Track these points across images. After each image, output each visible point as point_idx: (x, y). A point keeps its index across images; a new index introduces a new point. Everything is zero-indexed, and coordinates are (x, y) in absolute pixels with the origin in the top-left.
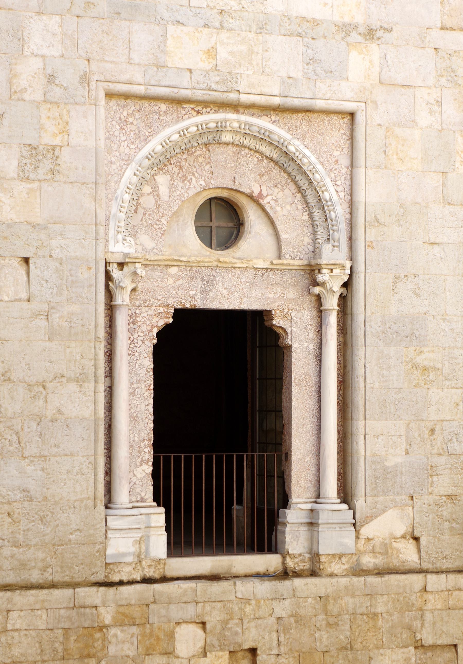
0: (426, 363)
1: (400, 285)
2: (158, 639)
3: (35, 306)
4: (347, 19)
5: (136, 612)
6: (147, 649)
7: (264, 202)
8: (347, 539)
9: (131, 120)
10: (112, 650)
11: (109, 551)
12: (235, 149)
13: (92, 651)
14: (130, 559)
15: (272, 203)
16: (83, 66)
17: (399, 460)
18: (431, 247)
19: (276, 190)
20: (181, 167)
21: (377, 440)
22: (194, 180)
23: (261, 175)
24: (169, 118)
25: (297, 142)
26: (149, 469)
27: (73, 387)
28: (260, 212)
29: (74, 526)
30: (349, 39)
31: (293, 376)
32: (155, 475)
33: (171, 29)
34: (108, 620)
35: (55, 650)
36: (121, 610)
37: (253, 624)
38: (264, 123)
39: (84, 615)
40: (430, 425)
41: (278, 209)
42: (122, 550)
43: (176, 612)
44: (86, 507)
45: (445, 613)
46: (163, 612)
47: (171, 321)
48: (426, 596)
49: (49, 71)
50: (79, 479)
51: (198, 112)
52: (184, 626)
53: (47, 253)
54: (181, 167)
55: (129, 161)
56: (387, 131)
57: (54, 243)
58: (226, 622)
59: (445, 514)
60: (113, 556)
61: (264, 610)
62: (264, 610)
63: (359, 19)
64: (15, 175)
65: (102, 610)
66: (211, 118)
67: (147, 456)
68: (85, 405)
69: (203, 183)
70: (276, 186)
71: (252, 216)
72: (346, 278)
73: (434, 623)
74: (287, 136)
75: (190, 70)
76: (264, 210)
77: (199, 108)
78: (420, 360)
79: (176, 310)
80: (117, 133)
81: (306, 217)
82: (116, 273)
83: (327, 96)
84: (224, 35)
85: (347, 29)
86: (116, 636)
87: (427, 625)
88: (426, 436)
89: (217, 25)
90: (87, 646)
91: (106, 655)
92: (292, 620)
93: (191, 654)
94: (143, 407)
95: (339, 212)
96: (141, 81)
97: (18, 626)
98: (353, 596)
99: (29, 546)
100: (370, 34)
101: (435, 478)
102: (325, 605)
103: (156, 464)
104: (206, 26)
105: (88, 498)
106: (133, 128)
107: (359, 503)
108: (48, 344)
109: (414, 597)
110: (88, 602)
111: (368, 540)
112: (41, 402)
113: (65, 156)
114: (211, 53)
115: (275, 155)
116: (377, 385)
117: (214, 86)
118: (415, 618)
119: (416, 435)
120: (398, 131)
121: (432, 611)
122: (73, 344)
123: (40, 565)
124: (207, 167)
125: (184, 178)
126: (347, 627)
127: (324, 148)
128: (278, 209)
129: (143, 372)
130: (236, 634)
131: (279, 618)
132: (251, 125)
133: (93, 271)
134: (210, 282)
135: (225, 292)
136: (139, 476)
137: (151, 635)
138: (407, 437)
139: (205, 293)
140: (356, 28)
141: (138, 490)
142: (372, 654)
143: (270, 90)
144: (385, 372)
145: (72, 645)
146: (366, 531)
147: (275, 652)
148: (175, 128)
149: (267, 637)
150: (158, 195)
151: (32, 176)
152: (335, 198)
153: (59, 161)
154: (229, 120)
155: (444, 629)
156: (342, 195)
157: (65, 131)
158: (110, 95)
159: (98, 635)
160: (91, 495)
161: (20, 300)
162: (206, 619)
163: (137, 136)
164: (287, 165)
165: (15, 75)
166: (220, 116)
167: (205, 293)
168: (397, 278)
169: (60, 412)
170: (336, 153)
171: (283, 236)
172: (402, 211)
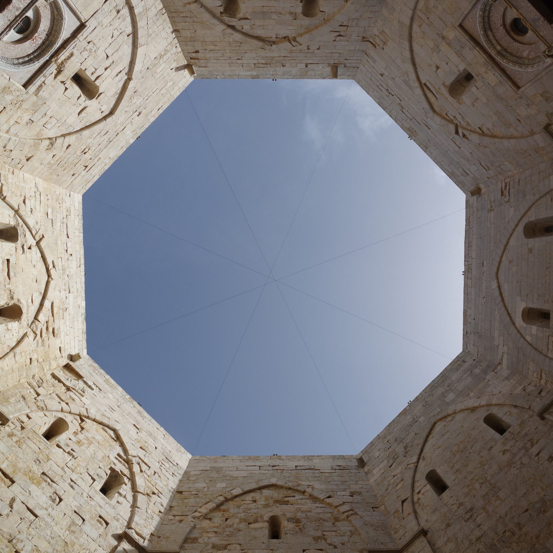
4: (448, 46)
63: (444, 43)
84: (480, 72)
85: (449, 44)
100: (443, 38)
140: (446, 43)
148: (510, 67)
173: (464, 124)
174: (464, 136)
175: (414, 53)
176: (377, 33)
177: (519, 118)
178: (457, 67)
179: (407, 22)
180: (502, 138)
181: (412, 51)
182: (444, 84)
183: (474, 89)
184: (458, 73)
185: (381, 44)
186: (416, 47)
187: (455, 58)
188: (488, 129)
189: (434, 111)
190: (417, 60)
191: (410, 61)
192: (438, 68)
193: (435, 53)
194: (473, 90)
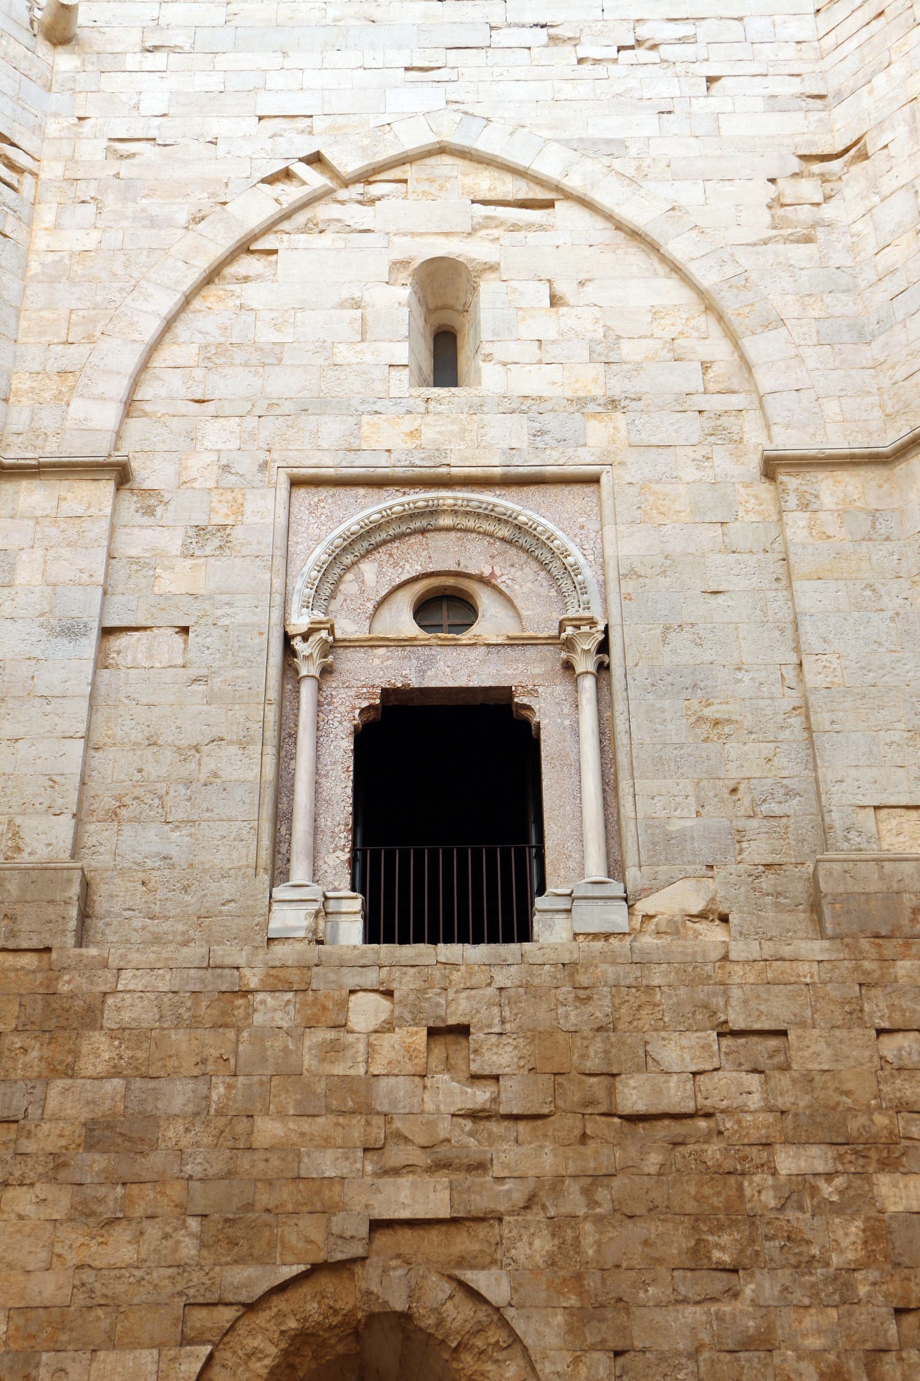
0: (718, 716)
1: (672, 635)
2: (324, 1008)
3: (192, 672)
4: (581, 394)
5: (294, 976)
6: (308, 1020)
7: (498, 582)
8: (616, 917)
9: (322, 504)
10: (258, 1019)
11: (272, 925)
12: (459, 534)
13: (228, 1020)
14: (302, 934)
15: (509, 582)
16: (262, 456)
17: (689, 823)
18: (714, 596)
19: (513, 570)
20: (391, 555)
21: (651, 799)
22: (407, 566)
23: (492, 557)
24: (368, 500)
25: (529, 513)
26: (346, 856)
27: (234, 749)
28: (496, 595)
29: (227, 896)
30: (585, 410)
31: (543, 754)
32: (353, 862)
33: (366, 418)
34: (253, 983)
35: (179, 1016)
36: (273, 972)
37: (464, 995)
38: (487, 497)
39: (221, 976)
40: (732, 784)
41: (517, 587)
42: (291, 923)
43: (351, 979)
44: (245, 876)
45: (761, 989)
46: (332, 976)
47: (378, 701)
48: (729, 967)
49: (224, 462)
50: (231, 837)
51: (404, 493)
52: (360, 994)
53: (210, 622)
54: (391, 555)
55: (318, 541)
56: (642, 488)
57: (219, 612)
58: (422, 991)
59: (764, 886)
60: (277, 930)
61: (480, 978)
62: (480, 978)
63: (598, 391)
64: (178, 553)
65: (246, 971)
66: (420, 497)
67: (343, 842)
68: (250, 768)
69: (419, 568)
70: (512, 566)
71: (485, 600)
72: (601, 637)
73: (746, 1002)
74: (518, 508)
75: (388, 451)
76: (501, 592)
77: (406, 490)
78: (707, 712)
79: (384, 690)
80: (305, 517)
81: (553, 593)
82: (298, 644)
83: (561, 462)
84: (429, 419)
86: (263, 1002)
87: (733, 1002)
88: (727, 796)
89: (423, 410)
90: (223, 1013)
91: (250, 1025)
92: (521, 990)
93: (371, 1028)
94: (339, 790)
95: (588, 574)
96: (331, 464)
97: (131, 987)
98: (614, 963)
99: (167, 918)
100: (613, 403)
101: (744, 845)
102: (572, 975)
103: (354, 850)
104: (409, 412)
105: (248, 866)
106: (325, 511)
107: (632, 873)
108: (206, 708)
109: (709, 967)
110: (228, 961)
111: (648, 917)
112: (193, 766)
113: (238, 534)
114: (414, 434)
115: (504, 532)
116: (648, 740)
117: (419, 463)
118: (715, 994)
119: (711, 794)
120: (654, 486)
121: (740, 985)
122: (237, 707)
123: (180, 938)
124: (425, 552)
125: (396, 565)
126: (607, 1001)
127: (565, 515)
128: (517, 587)
129: (339, 754)
130: (438, 1005)
131: (501, 989)
132: (469, 500)
133: (265, 636)
134: (430, 661)
135: (448, 670)
136: (331, 863)
137: (315, 1002)
138: (697, 797)
139: (422, 672)
140: (594, 399)
141: (330, 879)
142: (647, 1037)
143: (492, 461)
144: (658, 727)
145: (202, 1010)
146: (643, 906)
147: (497, 1029)
149: (483, 1010)
150: (363, 582)
151: (198, 553)
152: (582, 561)
153: (230, 538)
154: (442, 498)
155: (763, 1008)
156: (591, 558)
157: (239, 510)
158: (296, 483)
159: (240, 1002)
160: (252, 862)
161: (174, 667)
162: (394, 986)
163: (330, 518)
164: (523, 540)
165: (185, 468)
166: (432, 494)
167: (422, 672)
168: (667, 629)
169: (216, 775)
170: (580, 520)
171: (524, 613)
172: (669, 562)
173: (324, 211)
174: (287, 175)
175: (661, 269)
176: (828, 211)
177: (210, 408)
178: (505, 364)
179: (757, 347)
180: (187, 301)
181: (675, 269)
182: (493, 268)
183: (401, 352)
184: (486, 349)
185: (789, 190)
186: (672, 292)
187: (532, 381)
188: (246, 279)
189: (442, 150)
190: (635, 258)
191: (654, 233)
192: (555, 300)
193: (599, 335)
194: (399, 343)
